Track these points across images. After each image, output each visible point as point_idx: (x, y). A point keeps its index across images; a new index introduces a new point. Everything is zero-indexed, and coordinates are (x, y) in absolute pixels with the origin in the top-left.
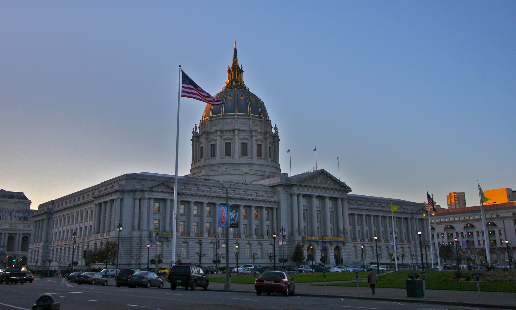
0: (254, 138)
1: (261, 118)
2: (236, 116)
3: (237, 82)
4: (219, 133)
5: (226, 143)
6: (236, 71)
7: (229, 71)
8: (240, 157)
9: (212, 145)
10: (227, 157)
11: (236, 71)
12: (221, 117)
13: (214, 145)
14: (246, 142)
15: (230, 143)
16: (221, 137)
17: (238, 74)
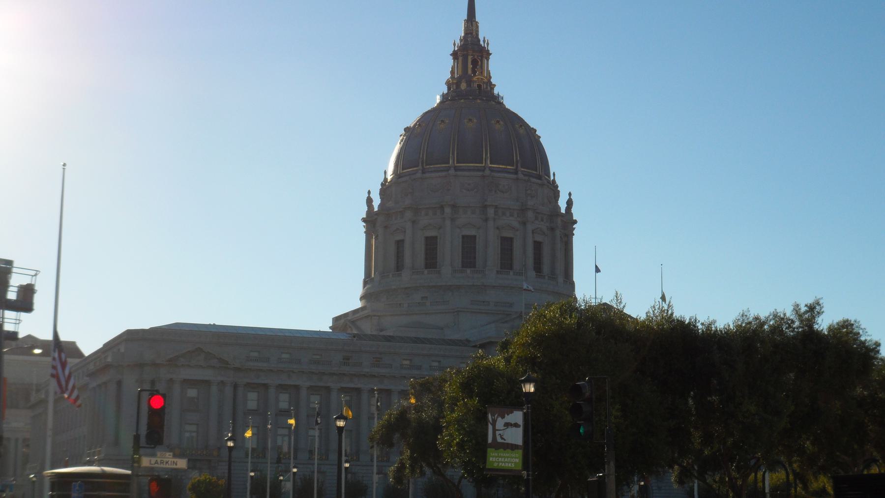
0: (530, 227)
1: (539, 177)
2: (487, 172)
3: (469, 82)
4: (448, 210)
5: (463, 237)
6: (471, 54)
7: (455, 55)
8: (497, 272)
9: (427, 238)
10: (469, 271)
11: (471, 54)
12: (452, 172)
13: (435, 238)
14: (508, 234)
15: (475, 237)
16: (453, 220)
17: (475, 63)
